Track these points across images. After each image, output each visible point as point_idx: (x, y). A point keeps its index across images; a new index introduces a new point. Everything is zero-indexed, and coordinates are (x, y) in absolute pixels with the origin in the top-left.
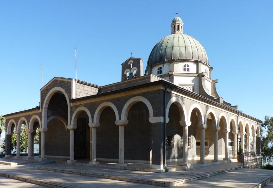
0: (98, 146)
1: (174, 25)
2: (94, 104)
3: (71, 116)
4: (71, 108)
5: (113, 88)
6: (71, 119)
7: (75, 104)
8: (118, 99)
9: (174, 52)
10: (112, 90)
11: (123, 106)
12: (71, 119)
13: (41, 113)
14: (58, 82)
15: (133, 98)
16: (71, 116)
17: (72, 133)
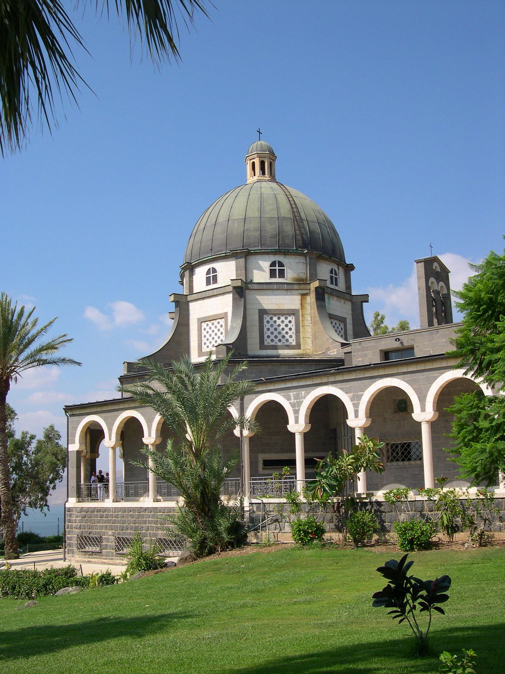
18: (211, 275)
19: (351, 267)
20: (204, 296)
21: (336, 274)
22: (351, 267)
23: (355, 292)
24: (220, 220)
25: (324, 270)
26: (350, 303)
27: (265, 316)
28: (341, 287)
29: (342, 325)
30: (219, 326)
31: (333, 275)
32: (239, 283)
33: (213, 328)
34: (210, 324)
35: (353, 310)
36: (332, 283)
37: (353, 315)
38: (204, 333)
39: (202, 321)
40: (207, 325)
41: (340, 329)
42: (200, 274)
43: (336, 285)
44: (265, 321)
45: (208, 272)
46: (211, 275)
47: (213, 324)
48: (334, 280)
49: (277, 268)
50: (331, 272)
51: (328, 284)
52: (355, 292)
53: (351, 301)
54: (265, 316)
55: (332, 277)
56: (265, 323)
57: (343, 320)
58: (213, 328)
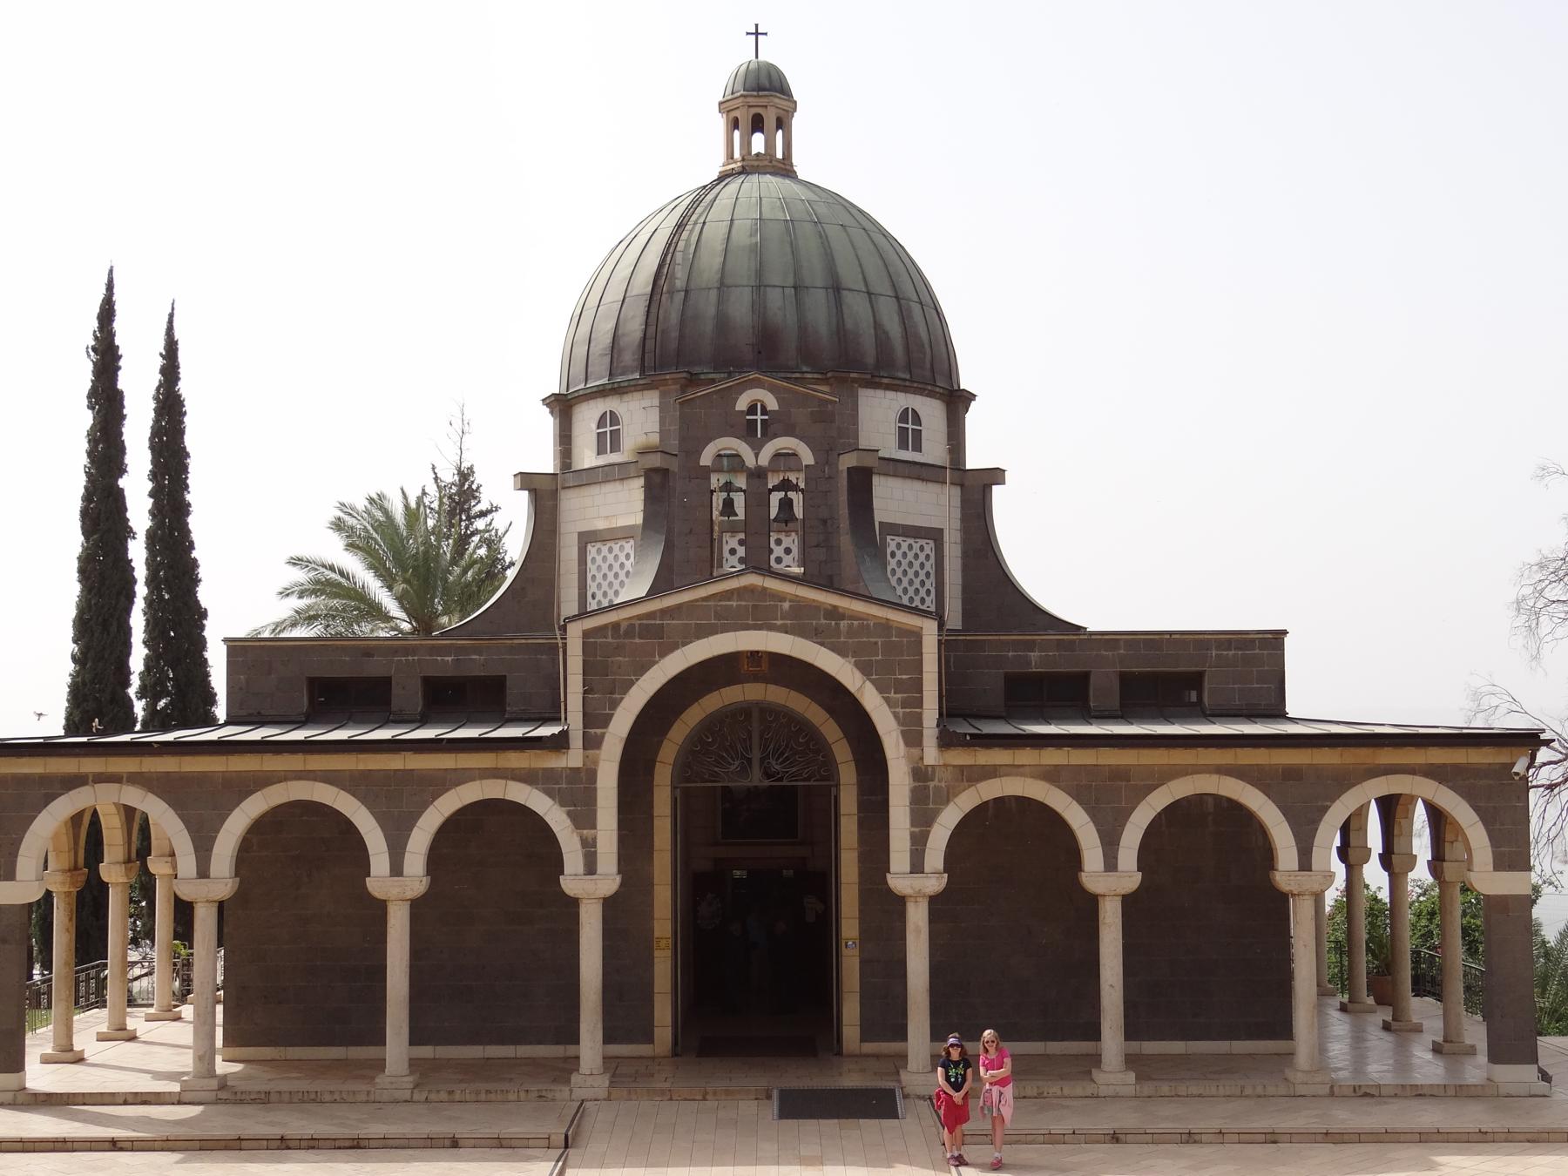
0: (936, 971)
1: (754, 111)
2: (1120, 774)
3: (923, 819)
4: (920, 774)
5: (1034, 655)
6: (919, 843)
7: (960, 757)
8: (1292, 774)
9: (849, 324)
10: (1029, 663)
11: (1326, 809)
12: (919, 843)
13: (588, 775)
14: (786, 605)
15: (1383, 778)
16: (923, 819)
17: (917, 917)
18: (608, 429)
19: (968, 398)
20: (594, 477)
21: (917, 419)
22: (968, 398)
23: (973, 461)
24: (634, 291)
25: (878, 416)
26: (957, 491)
27: (726, 537)
28: (934, 450)
29: (929, 547)
30: (622, 558)
31: (910, 426)
32: (656, 461)
33: (610, 557)
34: (605, 549)
35: (965, 503)
36: (903, 444)
37: (957, 524)
38: (592, 569)
39: (587, 538)
40: (599, 551)
41: (922, 557)
42: (587, 419)
43: (918, 448)
44: (726, 549)
45: (601, 422)
46: (608, 429)
47: (611, 550)
48: (909, 435)
49: (759, 417)
50: (904, 416)
51: (891, 449)
52: (973, 461)
53: (962, 486)
54: (726, 537)
55: (903, 432)
56: (726, 554)
57: (935, 535)
58: (610, 557)
